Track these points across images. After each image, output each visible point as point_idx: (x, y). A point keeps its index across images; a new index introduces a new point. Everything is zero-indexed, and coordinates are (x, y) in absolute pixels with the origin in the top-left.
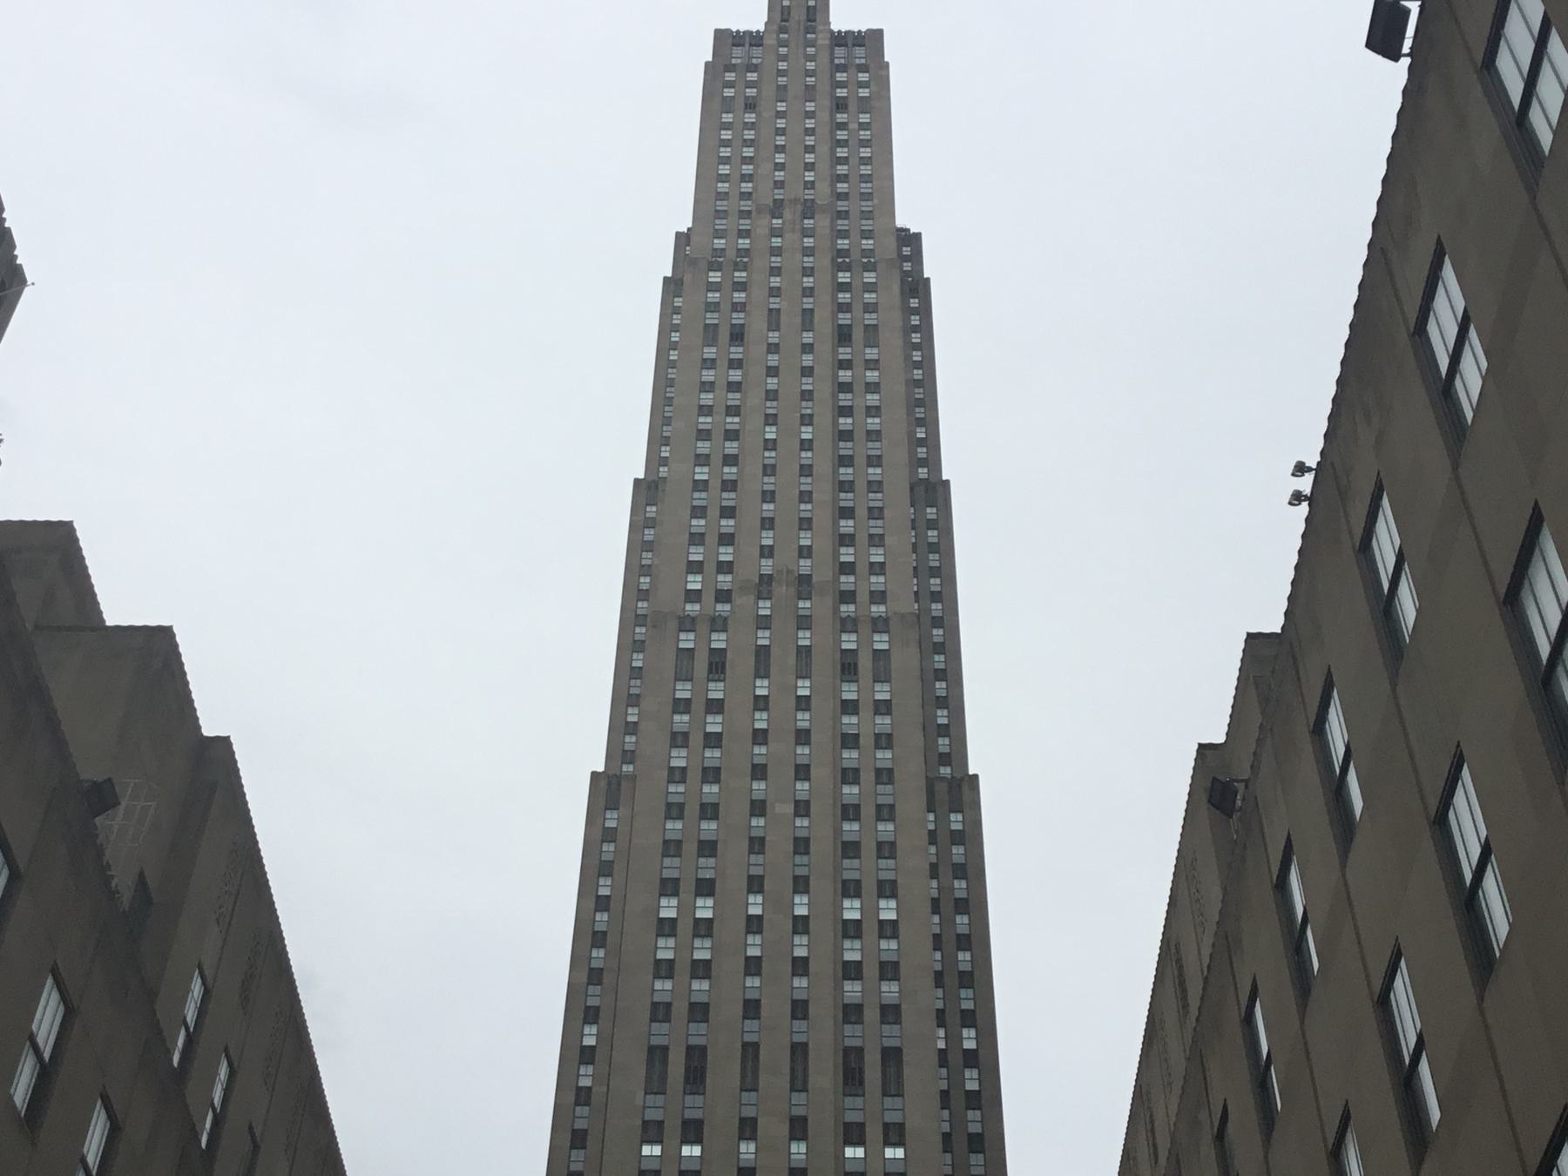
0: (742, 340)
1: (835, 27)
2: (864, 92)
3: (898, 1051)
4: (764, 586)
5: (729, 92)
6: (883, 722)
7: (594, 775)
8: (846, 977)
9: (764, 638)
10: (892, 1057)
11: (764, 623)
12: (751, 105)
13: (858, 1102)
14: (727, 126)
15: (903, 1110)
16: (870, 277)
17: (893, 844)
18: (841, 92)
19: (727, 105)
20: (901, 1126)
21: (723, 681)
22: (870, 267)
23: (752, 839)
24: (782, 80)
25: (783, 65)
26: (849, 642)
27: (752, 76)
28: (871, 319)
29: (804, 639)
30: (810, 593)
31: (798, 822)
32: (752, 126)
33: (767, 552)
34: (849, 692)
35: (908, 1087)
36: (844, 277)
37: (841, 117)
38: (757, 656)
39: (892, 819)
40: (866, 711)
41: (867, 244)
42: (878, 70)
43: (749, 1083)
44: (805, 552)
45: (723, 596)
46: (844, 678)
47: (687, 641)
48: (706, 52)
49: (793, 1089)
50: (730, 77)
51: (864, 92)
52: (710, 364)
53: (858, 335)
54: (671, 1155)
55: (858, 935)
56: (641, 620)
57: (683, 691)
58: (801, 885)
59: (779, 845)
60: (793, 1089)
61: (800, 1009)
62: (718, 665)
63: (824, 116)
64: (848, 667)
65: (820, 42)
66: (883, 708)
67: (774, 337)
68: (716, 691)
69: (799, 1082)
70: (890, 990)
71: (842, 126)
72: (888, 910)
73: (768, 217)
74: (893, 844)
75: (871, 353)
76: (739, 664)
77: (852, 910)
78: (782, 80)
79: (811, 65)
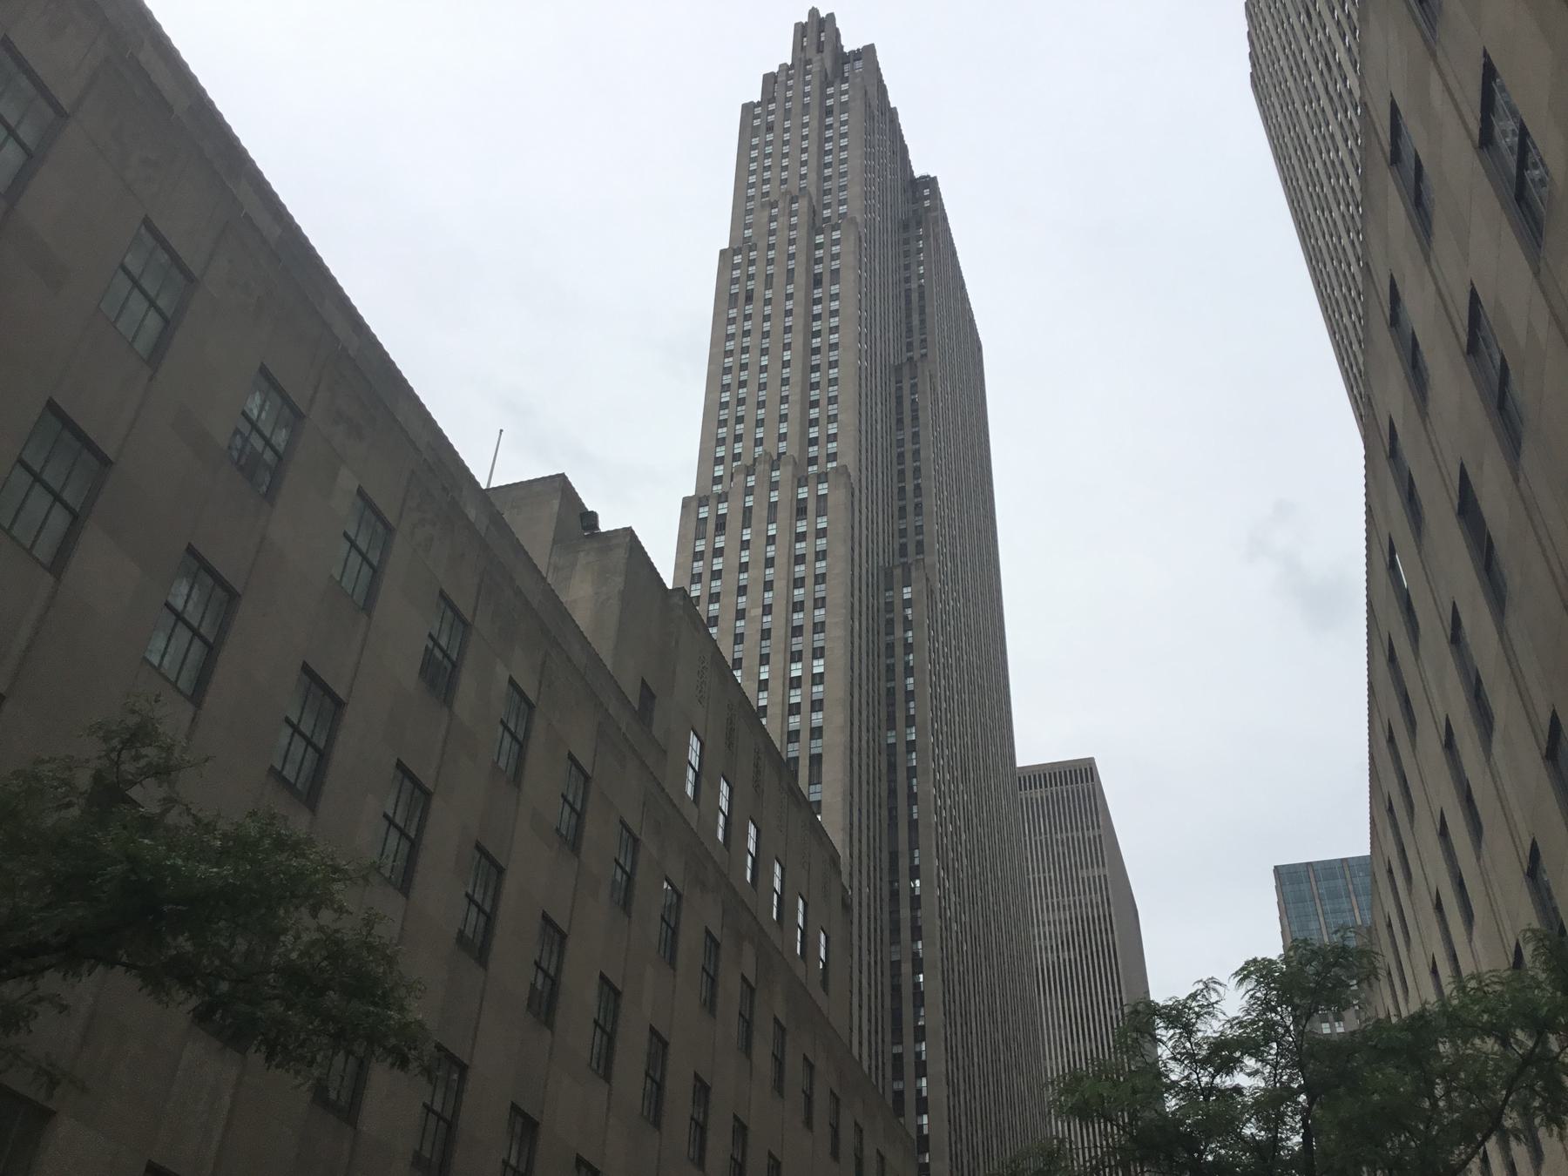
5: (757, 122)
16: (836, 235)
18: (829, 102)
22: (835, 228)
23: (736, 635)
30: (779, 465)
35: (825, 778)
38: (744, 512)
41: (843, 209)
58: (764, 660)
59: (752, 636)
64: (801, 510)
67: (769, 294)
72: (819, 667)
73: (768, 209)
77: (796, 670)
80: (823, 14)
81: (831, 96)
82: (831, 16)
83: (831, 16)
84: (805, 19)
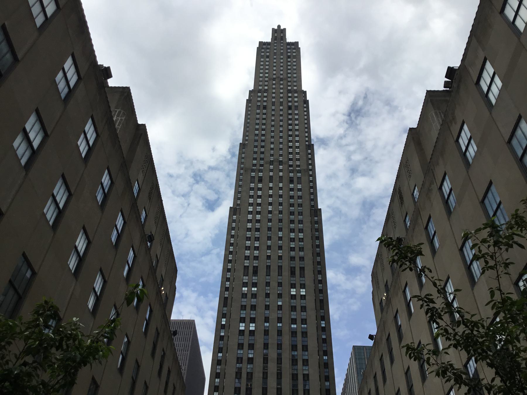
0: (266, 108)
1: (287, 41)
2: (294, 54)
3: (304, 268)
4: (271, 163)
5: (262, 54)
6: (300, 193)
7: (231, 208)
8: (291, 251)
9: (271, 174)
10: (302, 269)
11: (271, 170)
12: (268, 57)
13: (294, 279)
14: (262, 61)
15: (305, 281)
16: (296, 95)
17: (302, 221)
18: (289, 54)
19: (262, 57)
20: (304, 284)
21: (262, 183)
24: (275, 51)
25: (275, 48)
26: (291, 175)
27: (268, 50)
28: (296, 104)
29: (281, 174)
31: (280, 216)
32: (268, 61)
33: (272, 155)
34: (292, 186)
36: (290, 95)
37: (289, 60)
39: (302, 215)
40: (296, 191)
42: (298, 50)
43: (268, 274)
44: (281, 155)
45: (262, 165)
46: (290, 183)
47: (253, 174)
48: (257, 45)
49: (278, 276)
50: (263, 50)
51: (294, 54)
52: (258, 114)
53: (293, 108)
54: (249, 290)
55: (294, 241)
56: (242, 169)
57: (252, 185)
58: (280, 230)
59: (275, 220)
60: (278, 276)
61: (280, 258)
62: (260, 180)
63: (285, 59)
64: (291, 181)
65: (284, 43)
66: (300, 190)
67: (273, 108)
68: (260, 185)
69: (280, 274)
70: (301, 254)
71: (289, 62)
72: (301, 235)
73: (272, 81)
74: (302, 221)
75: (296, 112)
76: (266, 180)
77: (292, 235)
78: (275, 51)
79: (282, 48)
80: (282, 28)
81: (289, 52)
82: (285, 29)
83: (285, 29)
84: (276, 28)
